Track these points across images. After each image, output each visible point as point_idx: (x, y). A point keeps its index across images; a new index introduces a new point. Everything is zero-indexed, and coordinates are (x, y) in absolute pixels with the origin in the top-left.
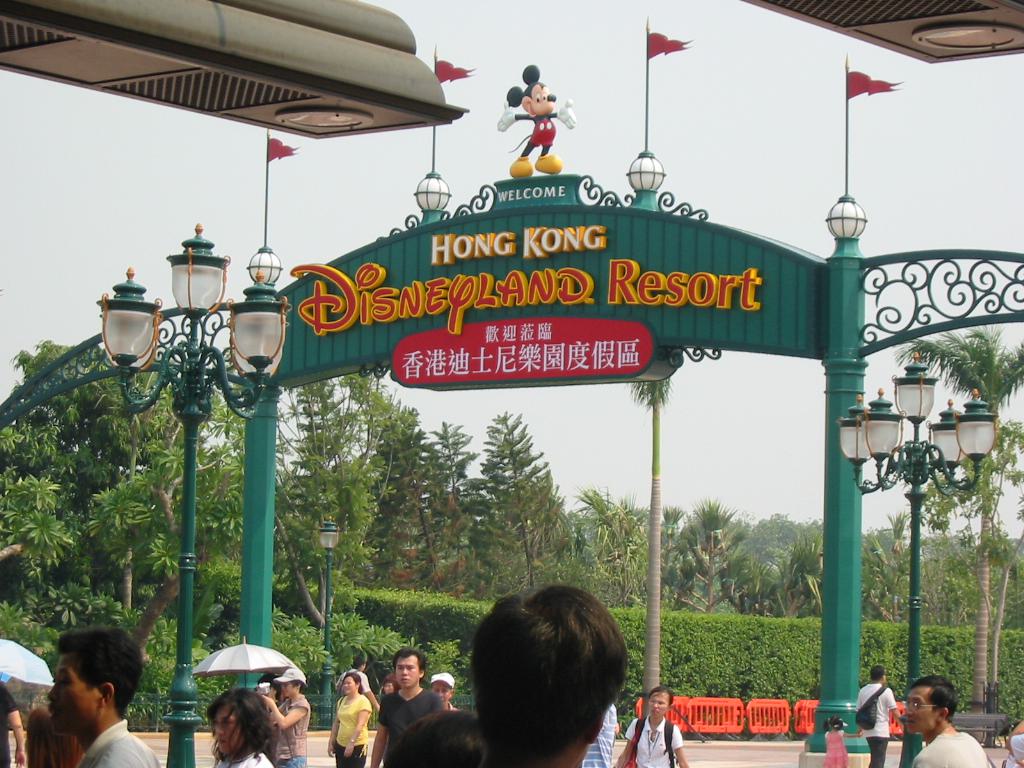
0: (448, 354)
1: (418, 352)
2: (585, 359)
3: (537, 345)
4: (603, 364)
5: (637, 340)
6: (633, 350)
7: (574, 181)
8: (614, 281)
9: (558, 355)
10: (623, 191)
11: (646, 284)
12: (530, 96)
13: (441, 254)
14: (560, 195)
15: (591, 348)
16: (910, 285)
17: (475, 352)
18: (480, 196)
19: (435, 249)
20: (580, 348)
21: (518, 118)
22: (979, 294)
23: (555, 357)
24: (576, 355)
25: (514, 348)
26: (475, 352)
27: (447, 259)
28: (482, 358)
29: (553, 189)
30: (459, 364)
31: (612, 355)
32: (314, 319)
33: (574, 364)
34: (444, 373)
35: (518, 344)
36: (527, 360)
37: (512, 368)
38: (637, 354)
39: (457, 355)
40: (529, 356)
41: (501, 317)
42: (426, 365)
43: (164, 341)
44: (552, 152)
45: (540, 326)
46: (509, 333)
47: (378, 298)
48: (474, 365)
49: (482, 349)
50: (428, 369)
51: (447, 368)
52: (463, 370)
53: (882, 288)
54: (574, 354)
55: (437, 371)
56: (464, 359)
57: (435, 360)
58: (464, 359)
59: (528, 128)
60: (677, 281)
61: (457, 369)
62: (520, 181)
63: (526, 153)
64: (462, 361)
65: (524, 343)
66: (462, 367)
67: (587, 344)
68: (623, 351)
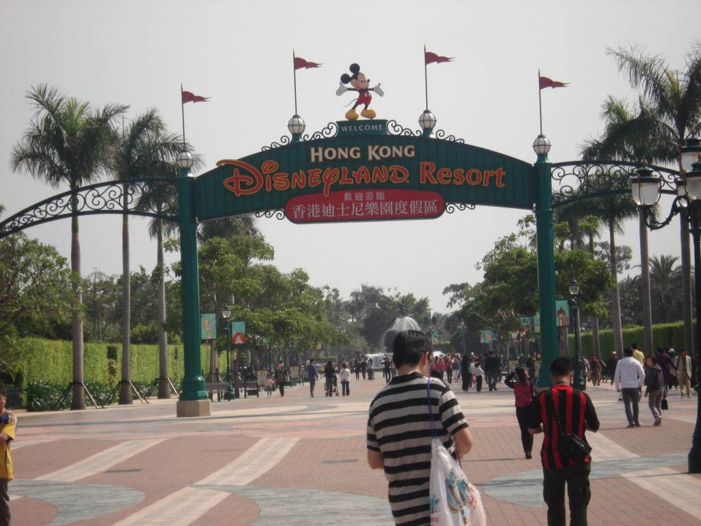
2: (405, 209)
4: (416, 212)
10: (416, 129)
13: (317, 157)
15: (409, 204)
16: (577, 175)
17: (337, 205)
18: (328, 128)
19: (313, 154)
20: (402, 204)
21: (349, 89)
25: (362, 204)
26: (337, 205)
27: (321, 159)
28: (343, 208)
29: (376, 126)
33: (398, 211)
34: (319, 216)
35: (365, 202)
41: (354, 188)
42: (307, 212)
43: (113, 197)
45: (377, 194)
46: (359, 196)
47: (277, 178)
49: (343, 204)
51: (321, 214)
53: (562, 177)
54: (398, 207)
59: (356, 95)
62: (352, 121)
66: (330, 213)
68: (427, 204)
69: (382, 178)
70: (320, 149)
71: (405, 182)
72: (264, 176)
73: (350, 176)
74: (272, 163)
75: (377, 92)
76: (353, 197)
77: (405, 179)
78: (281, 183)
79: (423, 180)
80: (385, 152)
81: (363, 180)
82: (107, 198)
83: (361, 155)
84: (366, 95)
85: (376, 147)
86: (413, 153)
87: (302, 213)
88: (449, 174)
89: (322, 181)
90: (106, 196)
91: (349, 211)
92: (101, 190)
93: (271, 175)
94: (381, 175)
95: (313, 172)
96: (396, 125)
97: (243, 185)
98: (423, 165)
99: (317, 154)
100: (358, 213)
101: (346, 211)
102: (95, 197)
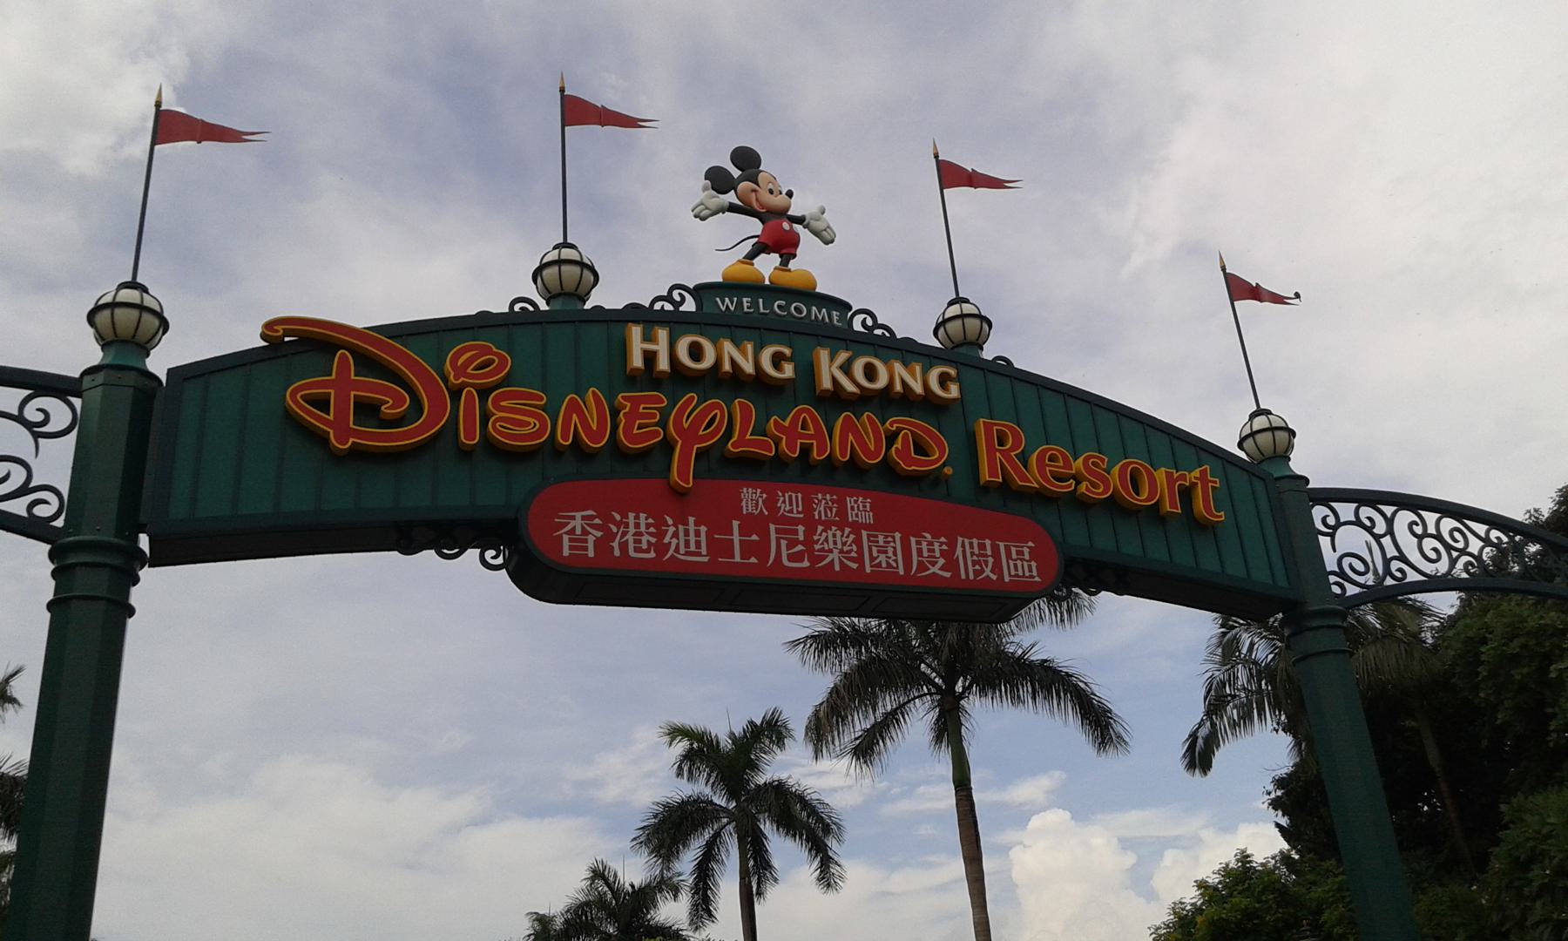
2: (941, 561)
3: (847, 530)
4: (977, 573)
6: (1027, 556)
9: (890, 550)
12: (758, 185)
13: (650, 357)
15: (952, 546)
17: (718, 526)
20: (930, 544)
21: (732, 208)
23: (886, 552)
24: (925, 554)
25: (801, 529)
26: (718, 526)
27: (663, 364)
28: (736, 538)
31: (991, 560)
32: (331, 417)
33: (922, 567)
34: (652, 555)
35: (811, 524)
36: (831, 551)
37: (802, 561)
38: (1034, 564)
39: (681, 528)
44: (793, 265)
45: (850, 501)
46: (790, 502)
47: (503, 404)
49: (736, 524)
50: (615, 544)
51: (661, 548)
52: (699, 554)
54: (920, 552)
55: (637, 550)
56: (697, 534)
57: (632, 530)
58: (697, 534)
61: (682, 550)
64: (692, 539)
65: (820, 522)
66: (693, 548)
67: (943, 539)
68: (1009, 556)
73: (761, 430)
75: (816, 233)
76: (771, 504)
80: (870, 373)
81: (806, 450)
85: (843, 356)
87: (591, 539)
91: (762, 549)
93: (484, 393)
95: (636, 402)
97: (368, 411)
100: (791, 558)
101: (747, 549)
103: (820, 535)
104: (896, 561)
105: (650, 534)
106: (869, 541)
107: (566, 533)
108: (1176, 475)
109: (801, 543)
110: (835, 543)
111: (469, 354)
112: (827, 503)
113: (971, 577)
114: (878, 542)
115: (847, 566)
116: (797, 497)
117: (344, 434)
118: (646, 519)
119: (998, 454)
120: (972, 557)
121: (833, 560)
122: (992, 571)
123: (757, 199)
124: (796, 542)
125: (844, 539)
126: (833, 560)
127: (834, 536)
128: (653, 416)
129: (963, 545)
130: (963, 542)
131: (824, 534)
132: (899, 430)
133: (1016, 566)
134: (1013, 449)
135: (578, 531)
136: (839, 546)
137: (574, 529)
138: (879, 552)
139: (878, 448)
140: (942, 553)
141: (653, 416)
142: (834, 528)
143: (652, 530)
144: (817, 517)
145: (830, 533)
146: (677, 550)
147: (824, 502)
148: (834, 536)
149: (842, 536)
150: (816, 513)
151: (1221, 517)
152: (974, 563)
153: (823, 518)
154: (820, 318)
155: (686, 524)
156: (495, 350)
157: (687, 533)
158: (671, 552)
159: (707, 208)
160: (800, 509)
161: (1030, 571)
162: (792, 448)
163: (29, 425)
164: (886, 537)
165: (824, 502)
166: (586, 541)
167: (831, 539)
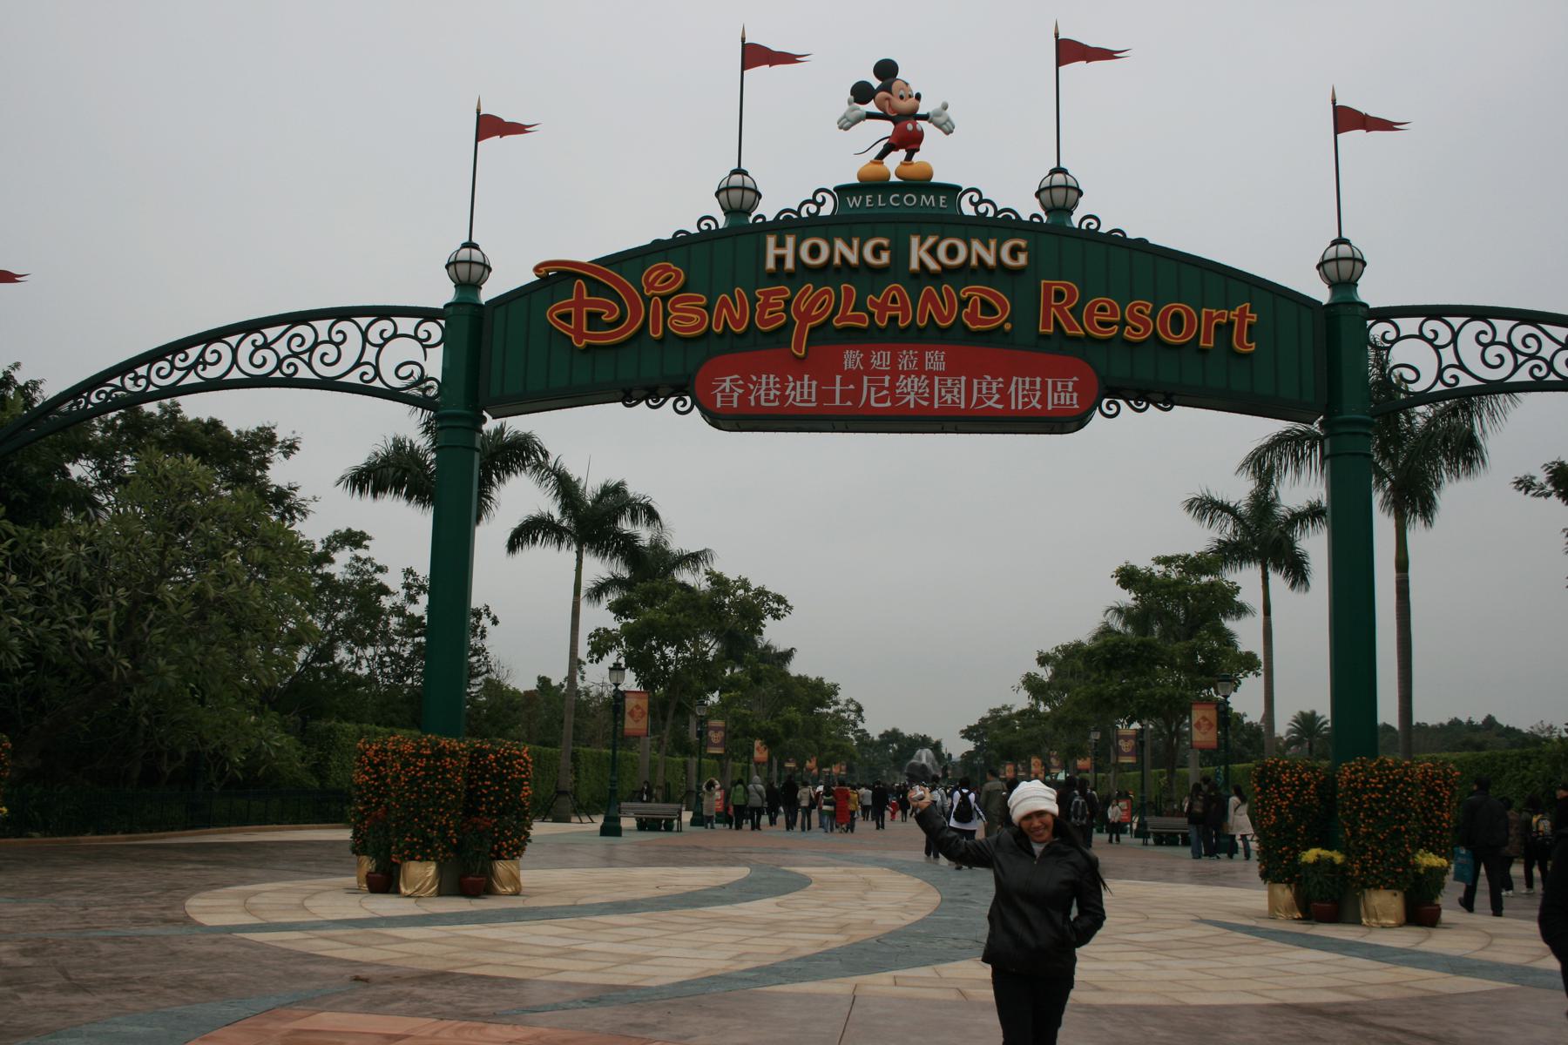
0: (783, 382)
1: (736, 376)
2: (997, 397)
3: (923, 377)
4: (1024, 404)
5: (1075, 379)
6: (1070, 389)
7: (953, 191)
8: (1048, 306)
9: (956, 390)
10: (1028, 208)
11: (1096, 312)
12: (891, 93)
13: (780, 260)
14: (941, 205)
15: (1008, 385)
16: (1430, 342)
17: (825, 379)
18: (813, 201)
19: (772, 251)
21: (870, 116)
22: (1521, 359)
24: (984, 391)
25: (887, 378)
26: (825, 379)
27: (789, 264)
28: (838, 388)
29: (932, 197)
30: (802, 394)
31: (1038, 394)
32: (572, 327)
33: (980, 402)
34: (777, 404)
35: (895, 373)
36: (909, 394)
37: (885, 402)
38: (1075, 395)
39: (798, 383)
40: (912, 391)
42: (749, 392)
44: (917, 158)
45: (928, 355)
46: (881, 359)
47: (678, 306)
48: (825, 395)
49: (838, 378)
50: (752, 398)
51: (783, 398)
52: (810, 401)
53: (1393, 342)
54: (980, 391)
55: (767, 401)
56: (810, 386)
57: (764, 387)
58: (810, 386)
59: (887, 128)
60: (1140, 311)
61: (798, 399)
62: (871, 185)
63: (882, 156)
64: (806, 391)
65: (903, 372)
66: (806, 397)
67: (1000, 379)
68: (1055, 389)
69: (940, 314)
70: (790, 241)
71: (1002, 325)
72: (647, 300)
74: (668, 269)
75: (939, 126)
76: (866, 361)
77: (1001, 319)
78: (687, 318)
79: (1046, 326)
80: (952, 252)
81: (893, 319)
82: (284, 352)
83: (891, 258)
84: (910, 127)
85: (930, 241)
86: (1022, 259)
87: (736, 395)
88: (1114, 314)
89: (790, 319)
90: (281, 347)
92: (271, 333)
94: (941, 307)
95: (767, 295)
96: (981, 201)
97: (594, 318)
98: (1048, 286)
99: (780, 252)
100: (877, 401)
102: (257, 348)
103: (902, 381)
104: (959, 398)
105: (776, 389)
106: (940, 384)
107: (720, 392)
108: (1215, 314)
109: (887, 389)
110: (913, 387)
111: (659, 271)
112: (910, 357)
113: (1020, 407)
114: (946, 384)
115: (920, 403)
116: (886, 354)
117: (580, 336)
118: (774, 378)
119: (1053, 309)
120: (1023, 391)
121: (909, 401)
122: (1038, 402)
123: (890, 105)
124: (883, 388)
125: (920, 384)
126: (910, 400)
127: (913, 382)
128: (779, 304)
129: (1017, 383)
130: (1017, 380)
131: (905, 381)
132: (969, 298)
133: (1059, 397)
134: (1066, 304)
135: (727, 390)
136: (916, 389)
137: (725, 388)
138: (946, 392)
139: (951, 313)
140: (999, 390)
141: (779, 304)
142: (913, 376)
143: (778, 386)
144: (900, 369)
145: (909, 380)
146: (794, 399)
147: (907, 356)
148: (913, 382)
149: (918, 382)
150: (900, 366)
151: (1251, 347)
152: (1024, 397)
153: (905, 368)
154: (928, 204)
155: (802, 379)
156: (673, 267)
157: (802, 386)
158: (790, 400)
159: (848, 120)
160: (888, 363)
161: (1071, 399)
162: (882, 319)
163: (421, 341)
164: (954, 380)
165: (907, 356)
166: (732, 396)
167: (909, 385)
